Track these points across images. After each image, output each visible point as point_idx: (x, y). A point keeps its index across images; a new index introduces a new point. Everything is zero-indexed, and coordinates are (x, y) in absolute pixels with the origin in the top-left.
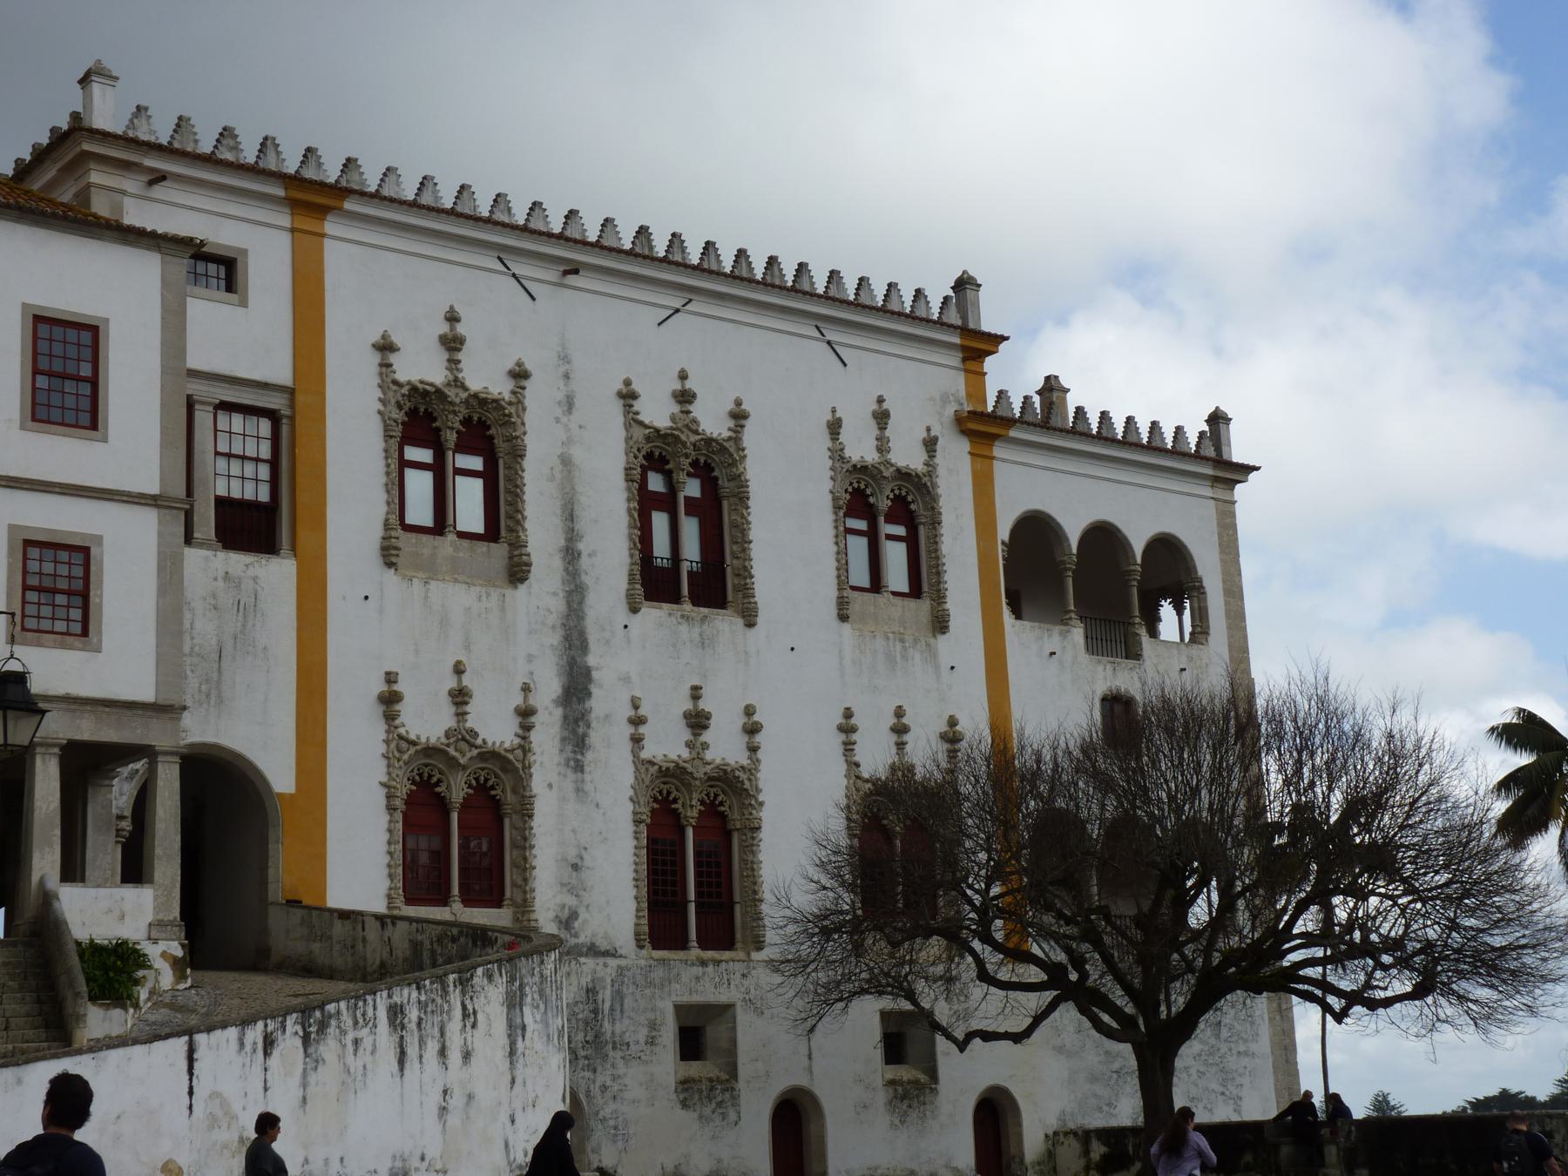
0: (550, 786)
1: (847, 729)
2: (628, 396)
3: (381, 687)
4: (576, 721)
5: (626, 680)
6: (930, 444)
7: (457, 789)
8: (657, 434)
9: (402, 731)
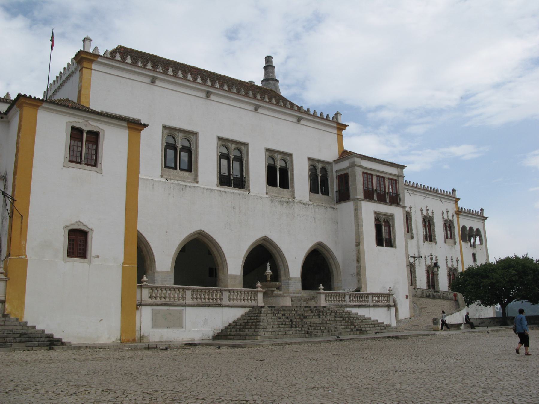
1: (447, 260)
2: (421, 210)
6: (453, 216)
8: (425, 216)
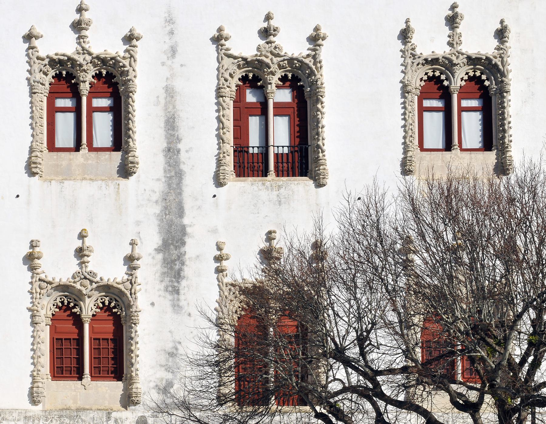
0: (153, 304)
3: (26, 250)
4: (173, 262)
5: (215, 231)
7: (88, 308)
9: (43, 276)
